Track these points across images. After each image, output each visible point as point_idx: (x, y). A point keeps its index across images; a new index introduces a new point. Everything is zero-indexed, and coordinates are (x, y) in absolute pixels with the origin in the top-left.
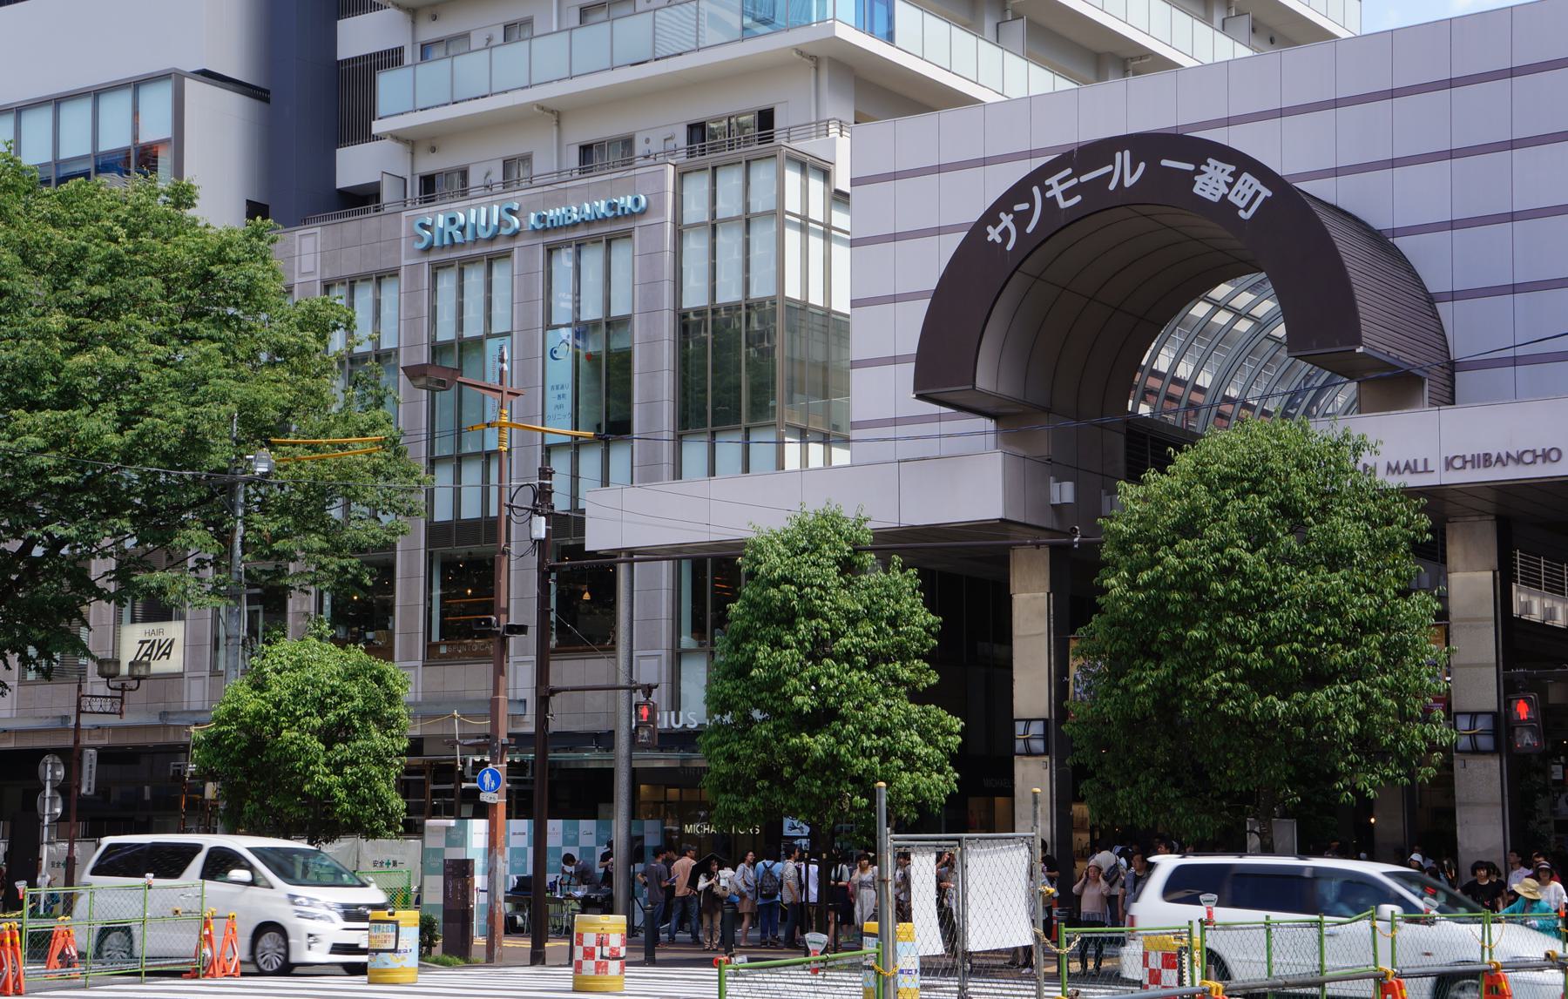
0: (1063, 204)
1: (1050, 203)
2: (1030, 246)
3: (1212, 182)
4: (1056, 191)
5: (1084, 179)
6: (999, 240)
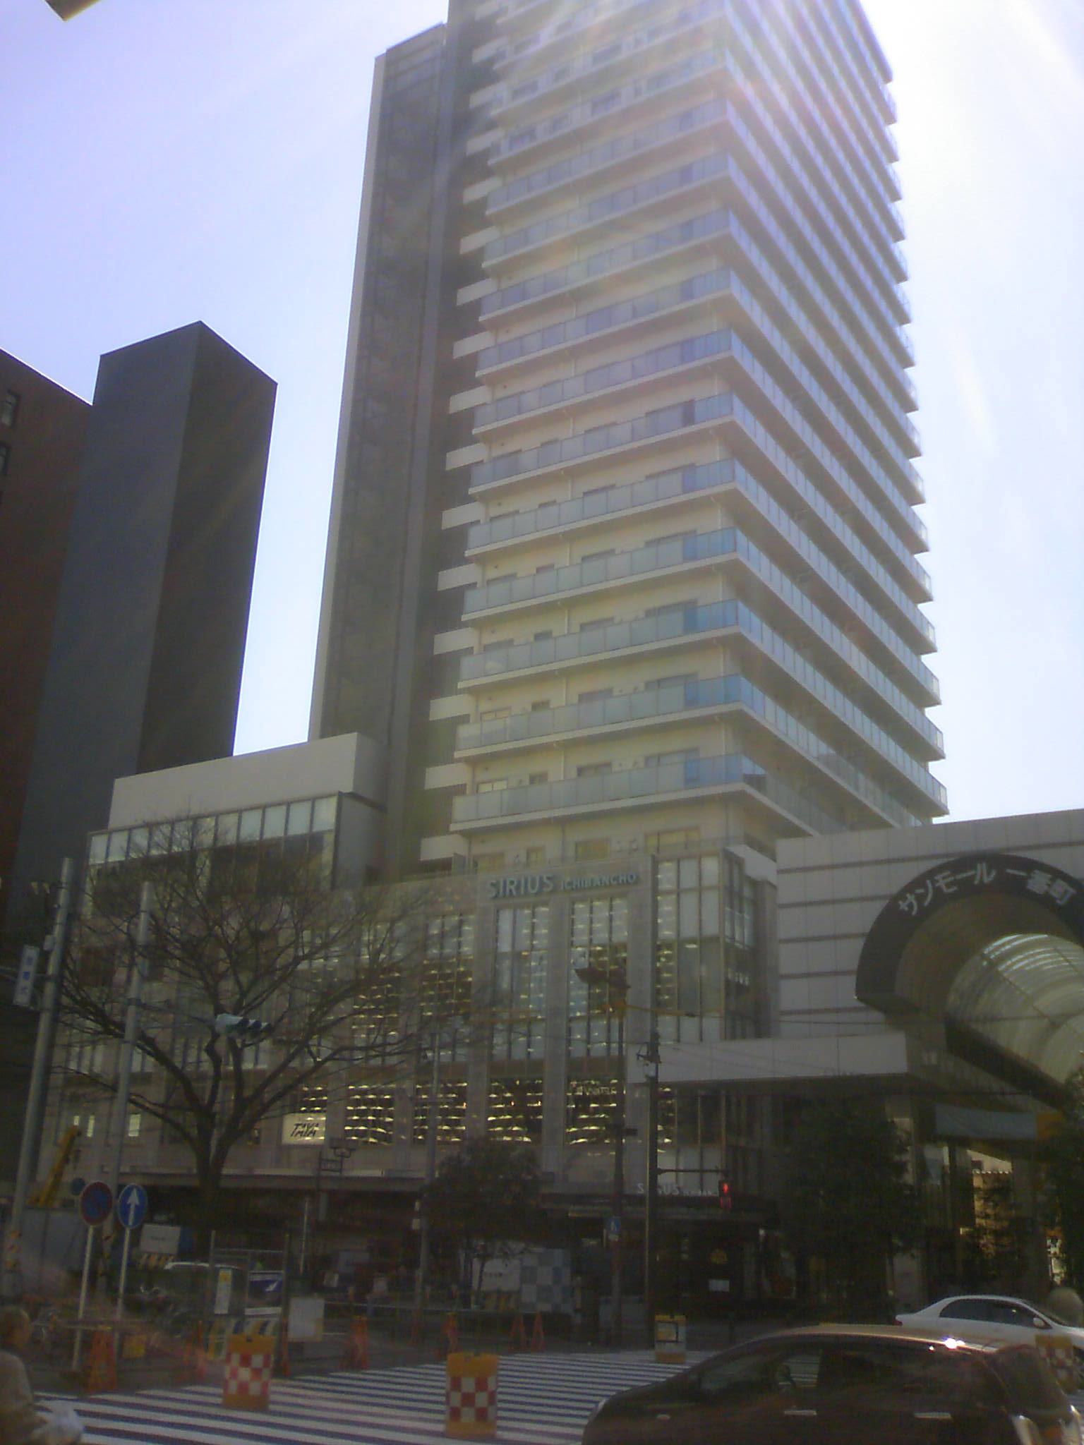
0: (945, 890)
1: (938, 891)
2: (925, 913)
3: (1038, 883)
4: (941, 883)
5: (959, 877)
6: (906, 909)
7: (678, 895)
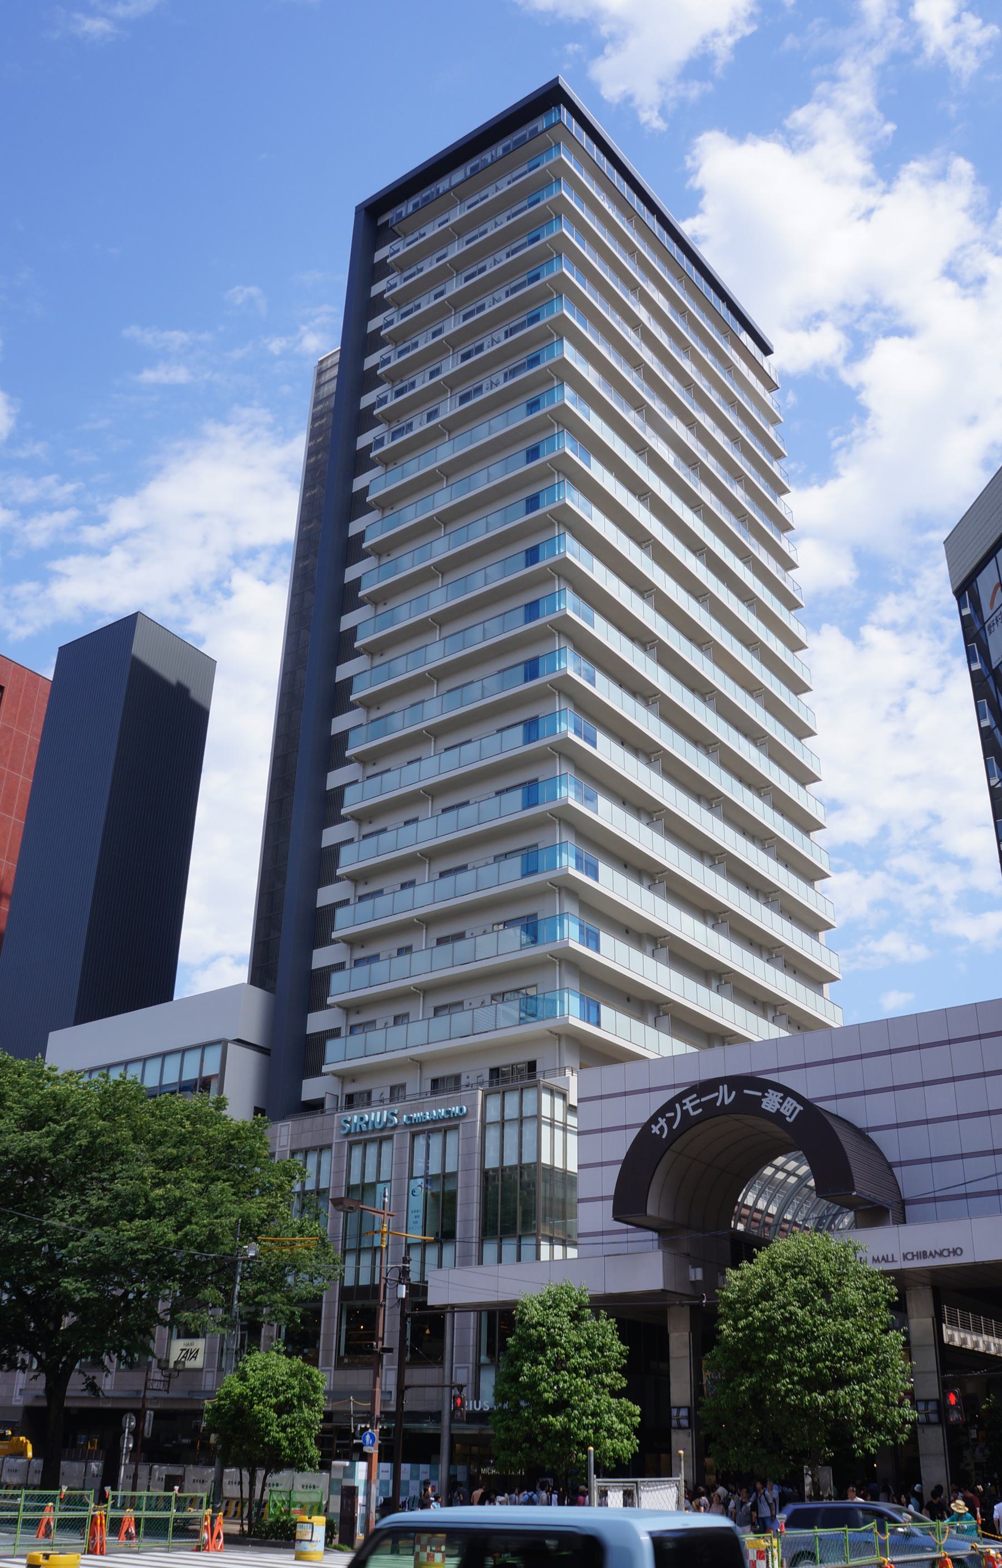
0: (692, 1113)
1: (685, 1113)
2: (675, 1136)
3: (771, 1102)
4: (689, 1106)
5: (703, 1100)
7: (521, 1121)
